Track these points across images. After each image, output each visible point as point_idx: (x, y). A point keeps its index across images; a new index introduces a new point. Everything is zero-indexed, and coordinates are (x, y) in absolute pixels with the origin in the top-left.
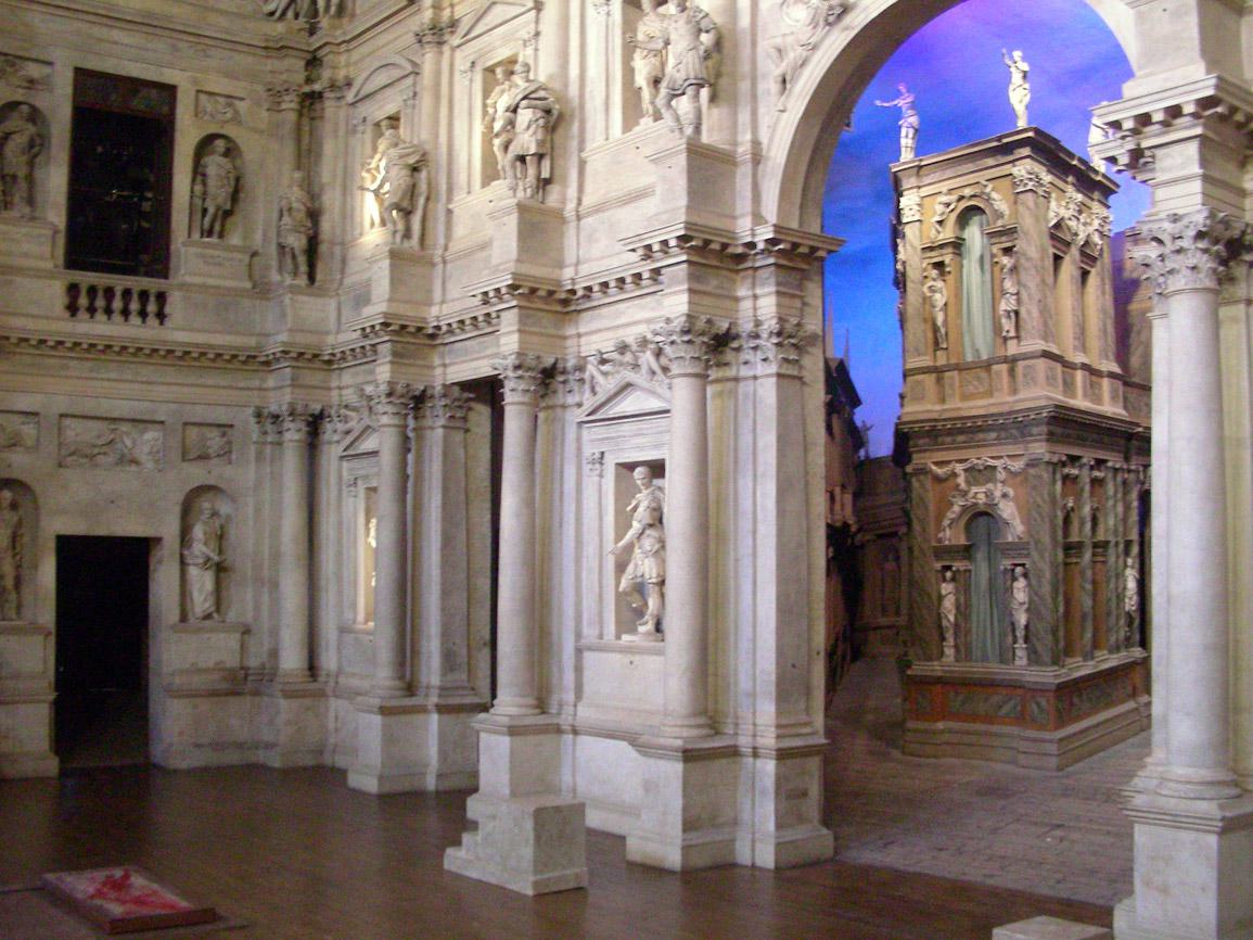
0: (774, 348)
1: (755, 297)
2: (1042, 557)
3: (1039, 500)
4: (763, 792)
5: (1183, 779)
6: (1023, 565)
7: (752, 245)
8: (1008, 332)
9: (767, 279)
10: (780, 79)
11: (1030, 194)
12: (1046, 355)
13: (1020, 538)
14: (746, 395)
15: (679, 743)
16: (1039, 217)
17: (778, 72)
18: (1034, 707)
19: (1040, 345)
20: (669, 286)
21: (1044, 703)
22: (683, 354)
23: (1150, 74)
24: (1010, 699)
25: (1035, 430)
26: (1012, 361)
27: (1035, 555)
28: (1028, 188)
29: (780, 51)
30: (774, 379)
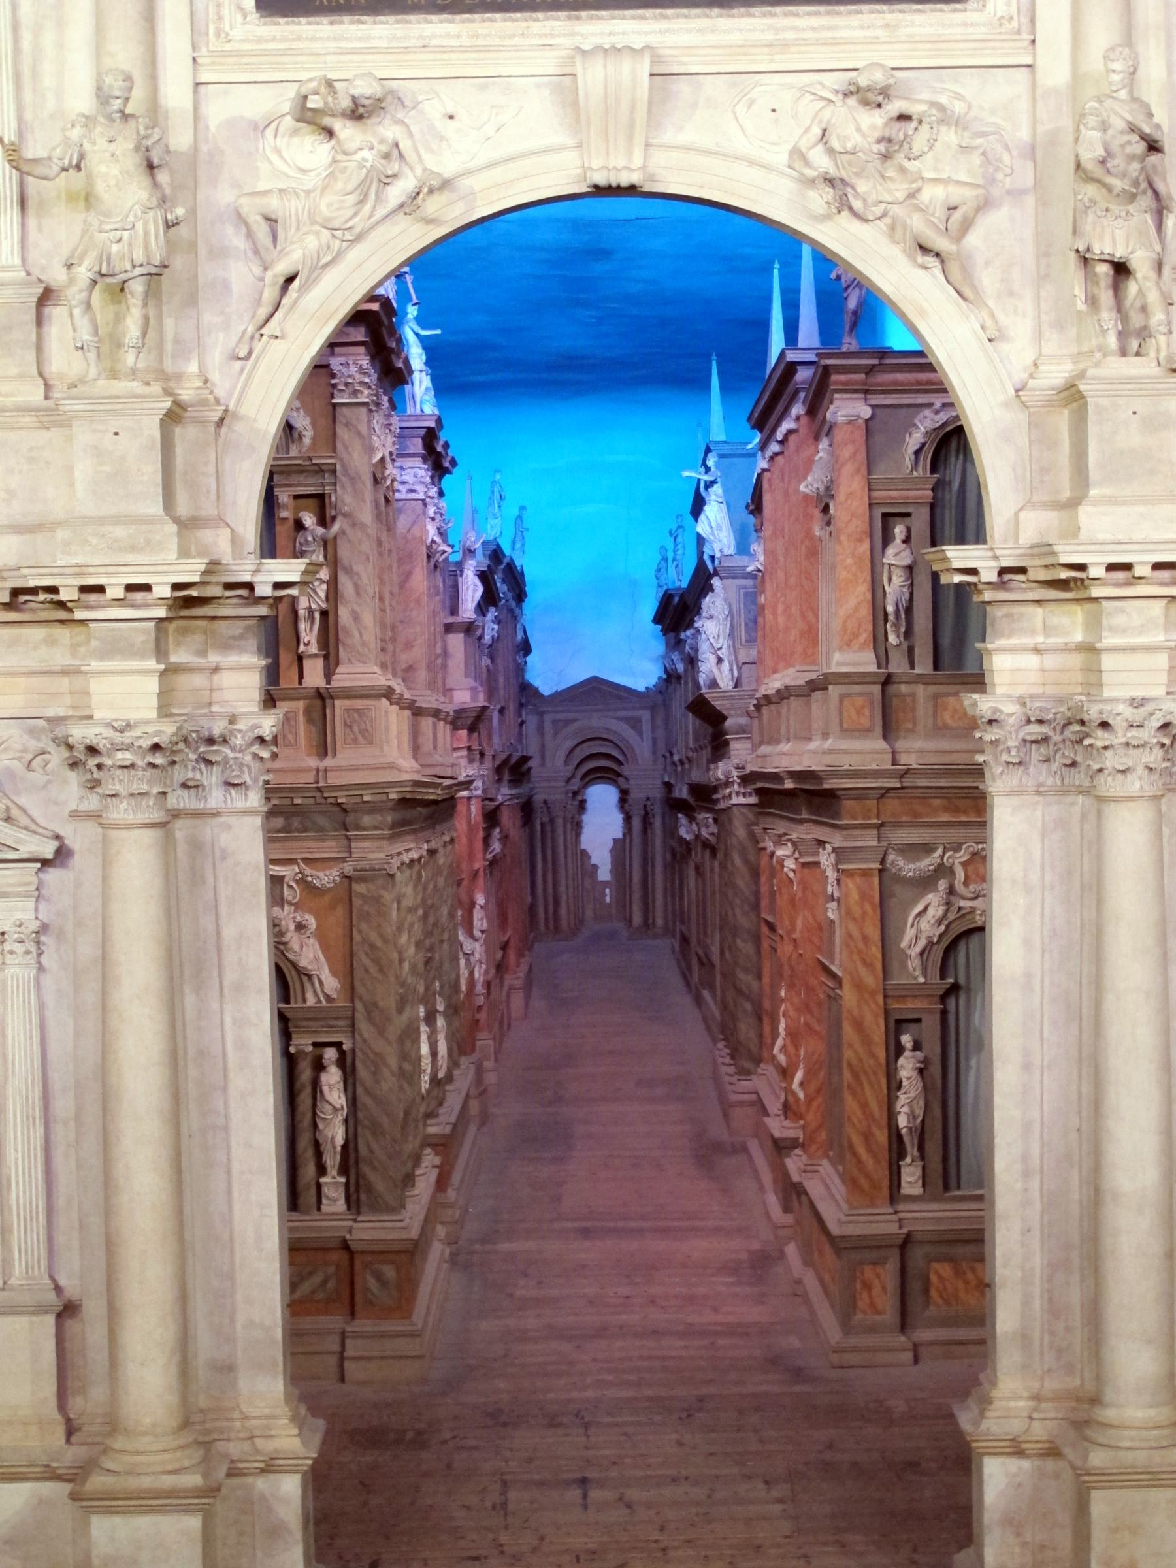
0: (256, 766)
1: (216, 669)
2: (381, 1033)
3: (374, 937)
4: (275, 1531)
5: (1151, 1425)
6: (338, 1045)
7: (250, 586)
8: (306, 645)
9: (241, 637)
10: (281, 280)
11: (363, 410)
12: (388, 693)
13: (329, 998)
14: (196, 846)
15: (193, 1480)
16: (371, 450)
17: (282, 268)
18: (372, 1283)
19: (379, 679)
20: (106, 653)
21: (389, 1272)
22: (144, 788)
23: (1113, 501)
24: (311, 1274)
25: (366, 820)
26: (322, 697)
27: (363, 1026)
28: (363, 399)
29: (271, 221)
30: (258, 821)
